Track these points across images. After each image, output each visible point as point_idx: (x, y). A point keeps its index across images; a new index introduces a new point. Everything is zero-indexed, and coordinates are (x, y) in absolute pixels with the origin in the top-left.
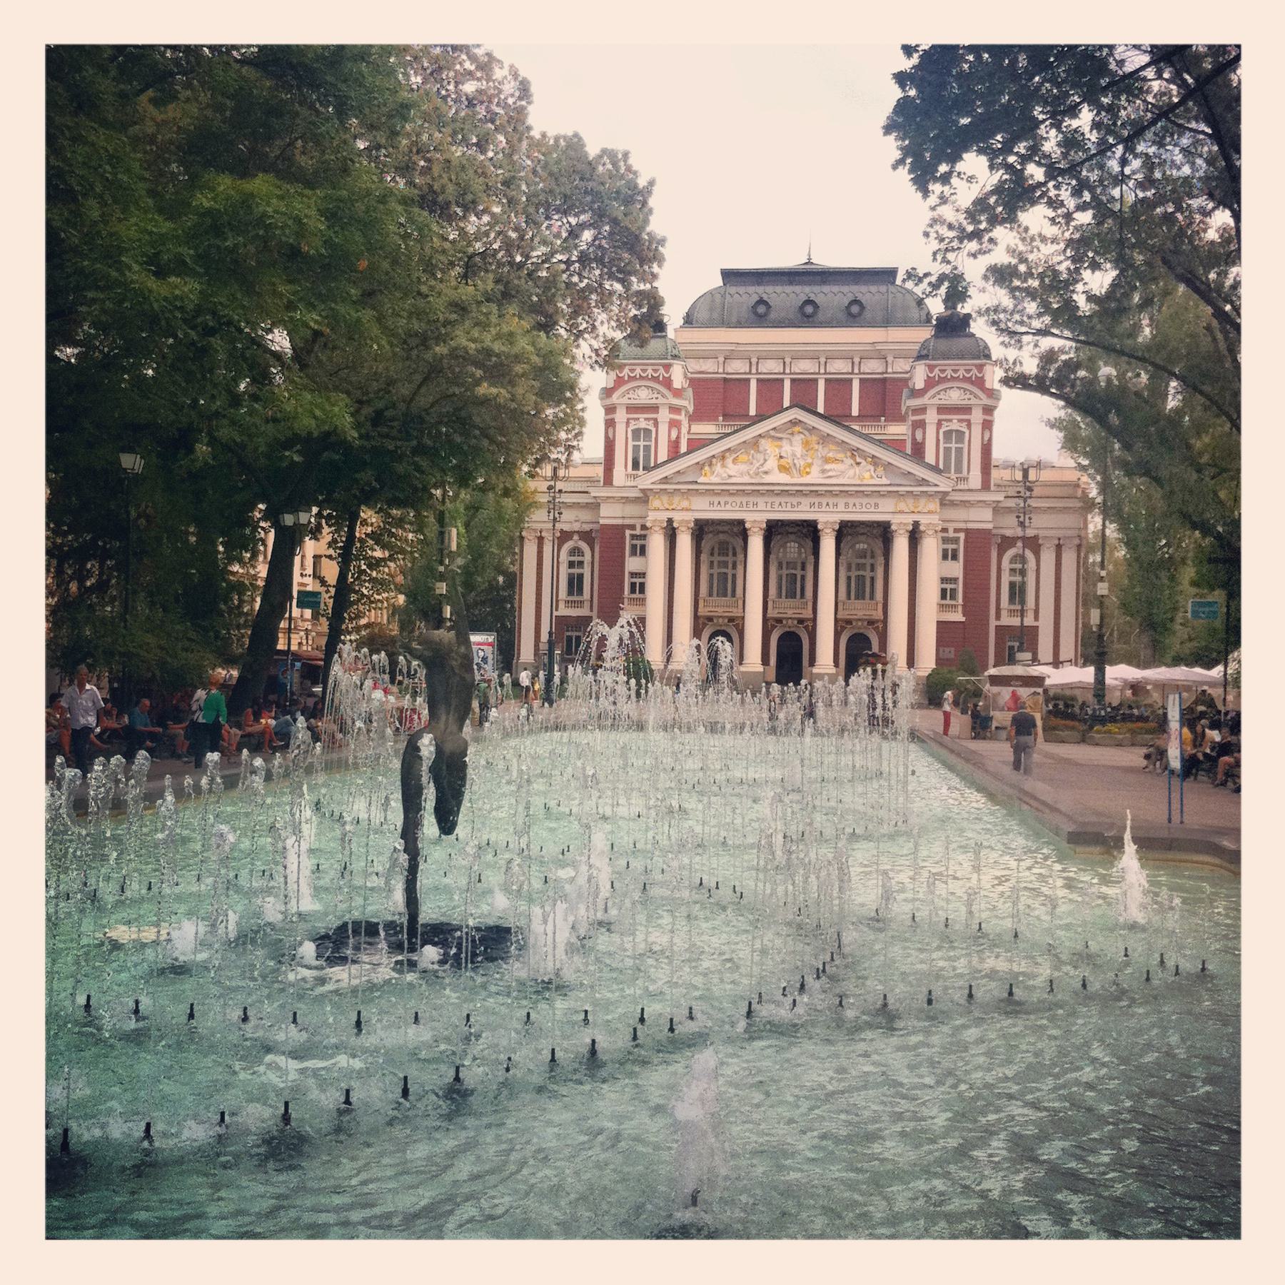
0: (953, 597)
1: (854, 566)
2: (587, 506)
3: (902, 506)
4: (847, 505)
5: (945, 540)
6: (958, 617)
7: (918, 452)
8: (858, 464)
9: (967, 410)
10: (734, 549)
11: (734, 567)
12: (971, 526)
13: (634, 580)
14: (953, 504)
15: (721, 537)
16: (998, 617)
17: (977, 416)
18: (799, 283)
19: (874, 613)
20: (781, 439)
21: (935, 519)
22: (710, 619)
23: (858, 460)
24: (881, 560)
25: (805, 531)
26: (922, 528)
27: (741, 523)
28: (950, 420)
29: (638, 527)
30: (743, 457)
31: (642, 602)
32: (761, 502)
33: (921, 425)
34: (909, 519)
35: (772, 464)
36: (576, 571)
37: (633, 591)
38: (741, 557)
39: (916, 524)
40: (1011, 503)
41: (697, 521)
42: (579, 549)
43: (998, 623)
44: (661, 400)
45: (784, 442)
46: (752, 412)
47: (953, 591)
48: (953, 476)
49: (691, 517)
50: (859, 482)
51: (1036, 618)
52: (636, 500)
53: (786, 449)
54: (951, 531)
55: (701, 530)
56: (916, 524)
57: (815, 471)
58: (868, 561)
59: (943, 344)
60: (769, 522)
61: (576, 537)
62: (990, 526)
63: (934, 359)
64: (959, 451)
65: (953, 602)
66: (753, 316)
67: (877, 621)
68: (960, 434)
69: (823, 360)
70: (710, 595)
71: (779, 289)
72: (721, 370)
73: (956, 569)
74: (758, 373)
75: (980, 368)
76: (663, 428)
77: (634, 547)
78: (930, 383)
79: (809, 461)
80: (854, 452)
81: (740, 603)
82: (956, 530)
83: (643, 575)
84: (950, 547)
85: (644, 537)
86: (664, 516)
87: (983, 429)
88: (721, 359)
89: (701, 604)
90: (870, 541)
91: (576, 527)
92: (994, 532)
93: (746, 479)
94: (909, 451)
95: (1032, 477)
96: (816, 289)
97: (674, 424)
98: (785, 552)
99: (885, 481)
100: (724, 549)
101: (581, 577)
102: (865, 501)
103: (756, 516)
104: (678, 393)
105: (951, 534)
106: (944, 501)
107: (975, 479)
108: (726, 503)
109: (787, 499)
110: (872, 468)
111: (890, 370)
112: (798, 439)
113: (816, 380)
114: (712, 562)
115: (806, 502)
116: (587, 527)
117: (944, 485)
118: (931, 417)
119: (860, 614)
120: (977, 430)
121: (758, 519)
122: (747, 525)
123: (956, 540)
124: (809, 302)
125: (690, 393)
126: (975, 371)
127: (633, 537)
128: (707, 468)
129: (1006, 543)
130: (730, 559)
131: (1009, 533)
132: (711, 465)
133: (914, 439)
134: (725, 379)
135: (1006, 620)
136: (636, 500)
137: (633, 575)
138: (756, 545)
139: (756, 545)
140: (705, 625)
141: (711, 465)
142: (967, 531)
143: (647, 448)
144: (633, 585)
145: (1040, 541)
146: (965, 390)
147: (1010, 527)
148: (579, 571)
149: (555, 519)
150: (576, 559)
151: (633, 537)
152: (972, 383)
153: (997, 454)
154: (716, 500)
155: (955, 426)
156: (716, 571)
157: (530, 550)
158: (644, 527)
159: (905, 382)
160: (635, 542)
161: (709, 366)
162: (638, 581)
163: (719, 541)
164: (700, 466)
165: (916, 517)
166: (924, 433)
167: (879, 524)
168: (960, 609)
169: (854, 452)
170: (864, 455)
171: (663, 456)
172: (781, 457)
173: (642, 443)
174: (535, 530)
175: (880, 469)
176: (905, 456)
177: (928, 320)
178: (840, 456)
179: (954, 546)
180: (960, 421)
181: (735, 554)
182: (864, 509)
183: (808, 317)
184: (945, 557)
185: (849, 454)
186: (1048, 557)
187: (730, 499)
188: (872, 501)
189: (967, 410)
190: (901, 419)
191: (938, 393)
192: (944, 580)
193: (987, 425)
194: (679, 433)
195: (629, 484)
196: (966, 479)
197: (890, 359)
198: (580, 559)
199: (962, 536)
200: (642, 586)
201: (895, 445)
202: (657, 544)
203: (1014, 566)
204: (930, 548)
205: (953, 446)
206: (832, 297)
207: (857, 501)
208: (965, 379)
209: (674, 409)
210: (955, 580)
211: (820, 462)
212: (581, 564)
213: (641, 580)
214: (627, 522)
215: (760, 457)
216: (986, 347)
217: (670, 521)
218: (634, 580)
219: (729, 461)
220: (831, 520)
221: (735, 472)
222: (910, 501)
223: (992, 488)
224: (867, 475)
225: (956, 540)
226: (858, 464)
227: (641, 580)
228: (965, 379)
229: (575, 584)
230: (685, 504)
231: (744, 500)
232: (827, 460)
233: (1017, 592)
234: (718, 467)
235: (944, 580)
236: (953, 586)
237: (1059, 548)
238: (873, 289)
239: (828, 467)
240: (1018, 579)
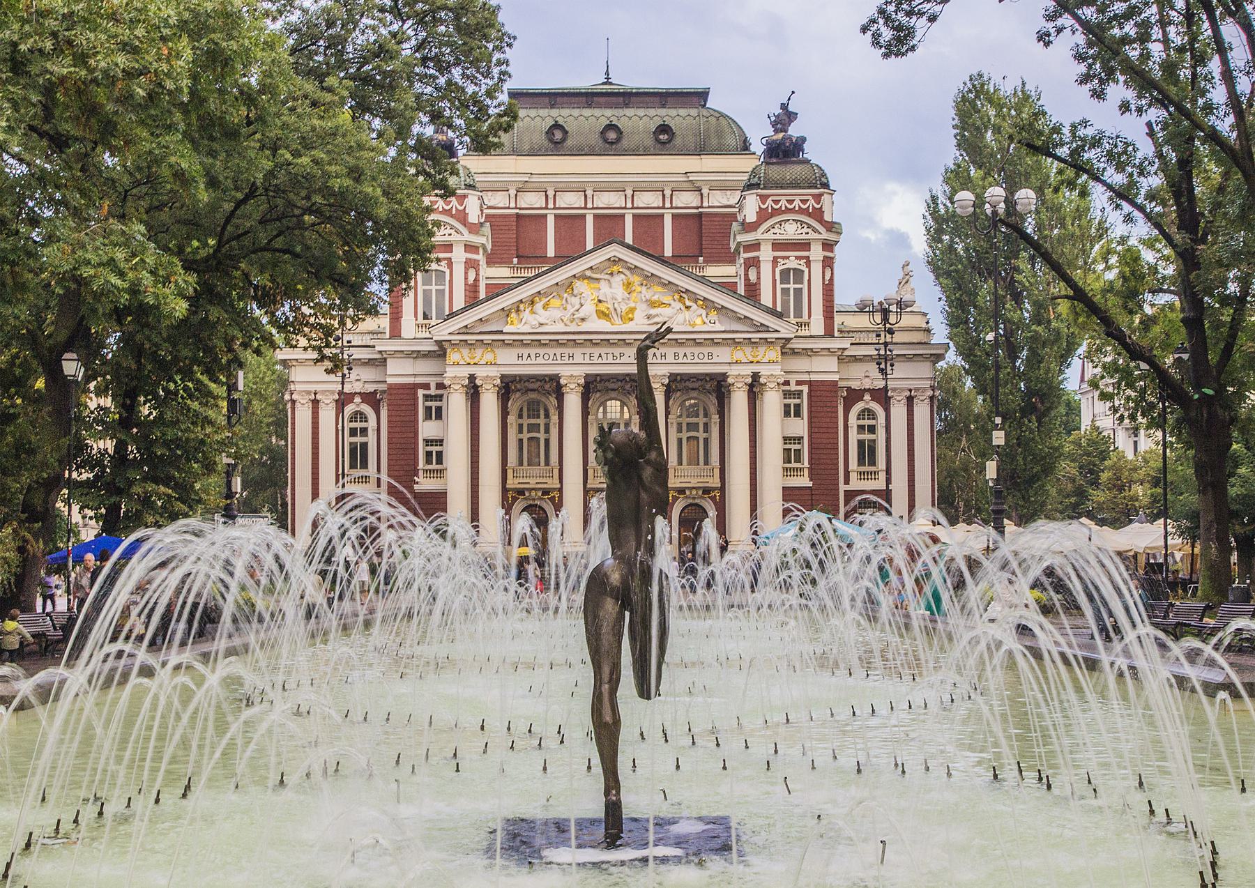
0: (798, 460)
1: (684, 428)
2: (369, 363)
3: (739, 355)
4: (676, 355)
5: (787, 394)
6: (804, 481)
7: (752, 293)
8: (688, 308)
9: (806, 245)
10: (547, 411)
11: (547, 431)
12: (814, 377)
13: (429, 449)
14: (794, 352)
15: (533, 396)
16: (847, 482)
17: (817, 253)
18: (600, 106)
19: (710, 480)
20: (598, 280)
21: (776, 370)
22: (521, 492)
23: (688, 303)
24: (715, 418)
25: (628, 387)
26: (762, 380)
27: (555, 379)
28: (788, 258)
29: (433, 386)
30: (555, 302)
31: (441, 473)
33: (754, 263)
34: (748, 370)
35: (589, 309)
36: (359, 439)
37: (429, 461)
38: (554, 418)
39: (755, 376)
40: (871, 351)
41: (503, 377)
42: (362, 414)
43: (848, 488)
44: (455, 237)
45: (602, 282)
46: (551, 253)
47: (798, 452)
48: (792, 320)
49: (495, 372)
50: (691, 329)
51: (888, 481)
52: (427, 355)
53: (605, 290)
54: (793, 383)
55: (508, 387)
56: (755, 376)
57: (639, 316)
58: (701, 420)
59: (776, 171)
60: (587, 376)
61: (358, 400)
62: (835, 377)
63: (764, 188)
64: (798, 292)
65: (798, 465)
66: (546, 143)
67: (714, 489)
68: (798, 273)
69: (629, 193)
70: (521, 464)
71: (576, 112)
72: (512, 205)
73: (800, 427)
74: (555, 208)
75: (818, 198)
76: (459, 270)
77: (428, 409)
78: (763, 216)
79: (632, 305)
80: (682, 293)
81: (556, 472)
82: (799, 383)
83: (440, 442)
84: (793, 402)
85: (439, 398)
86: (465, 372)
87: (824, 268)
88: (512, 192)
89: (510, 473)
90: (702, 396)
91: (358, 387)
92: (841, 384)
93: (560, 327)
94: (741, 290)
95: (892, 319)
96: (620, 112)
97: (470, 264)
98: (605, 412)
99: (718, 327)
100: (533, 409)
101: (364, 446)
102: (696, 350)
103: (572, 370)
104: (474, 229)
105: (793, 387)
106: (787, 349)
107: (817, 327)
109: (610, 350)
110: (704, 313)
111: (705, 204)
112: (618, 279)
113: (623, 216)
114: (521, 426)
116: (370, 388)
117: (785, 330)
118: (766, 254)
119: (694, 482)
120: (817, 268)
122: (562, 381)
123: (799, 394)
124: (611, 127)
125: (487, 229)
126: (812, 202)
127: (427, 397)
128: (513, 315)
129: (854, 396)
130: (541, 421)
131: (855, 385)
132: (518, 311)
133: (747, 279)
134: (518, 216)
135: (855, 484)
136: (427, 355)
137: (428, 442)
139: (573, 402)
140: (514, 499)
141: (518, 311)
142: (810, 383)
143: (440, 293)
144: (429, 454)
145: (890, 394)
147: (865, 376)
148: (363, 439)
149: (343, 376)
150: (358, 425)
151: (427, 397)
152: (809, 215)
153: (844, 298)
154: (525, 351)
155: (793, 264)
156: (525, 436)
157: (303, 416)
158: (440, 386)
159: (733, 217)
160: (429, 404)
161: (498, 200)
162: (434, 449)
163: (529, 396)
164: (506, 312)
165: (756, 368)
166: (759, 273)
167: (711, 377)
168: (806, 472)
169: (682, 293)
170: (695, 298)
171: (459, 303)
172: (600, 301)
173: (434, 288)
174: (309, 393)
175: (713, 315)
176: (740, 298)
177: (745, 147)
178: (667, 299)
179: (797, 401)
180: (797, 258)
181: (547, 416)
183: (612, 143)
184: (787, 413)
185: (677, 297)
186: (899, 411)
187: (542, 351)
188: (706, 350)
189: (806, 245)
190: (730, 259)
192: (786, 440)
193: (828, 263)
194: (477, 274)
195: (420, 335)
196: (807, 324)
197: (705, 191)
198: (363, 425)
199: (805, 388)
200: (439, 454)
201: (728, 288)
202: (457, 404)
203: (861, 422)
204: (772, 402)
205: (792, 286)
206: (639, 121)
207: (688, 350)
208: (801, 211)
209: (469, 248)
210: (799, 440)
211: (644, 306)
212: (364, 431)
213: (439, 448)
214: (419, 380)
215: (575, 301)
216: (824, 175)
217: (472, 378)
218: (429, 449)
219: (539, 306)
220: (659, 373)
221: (548, 318)
222: (748, 350)
223: (836, 334)
224: (699, 321)
225: (799, 394)
226: (688, 308)
227: (439, 448)
228: (801, 211)
229: (359, 456)
230: (489, 357)
231: (558, 351)
232: (652, 304)
233: (867, 453)
234: (526, 315)
235: (786, 440)
236: (797, 447)
237: (910, 400)
238: (683, 112)
239: (653, 311)
240: (867, 436)
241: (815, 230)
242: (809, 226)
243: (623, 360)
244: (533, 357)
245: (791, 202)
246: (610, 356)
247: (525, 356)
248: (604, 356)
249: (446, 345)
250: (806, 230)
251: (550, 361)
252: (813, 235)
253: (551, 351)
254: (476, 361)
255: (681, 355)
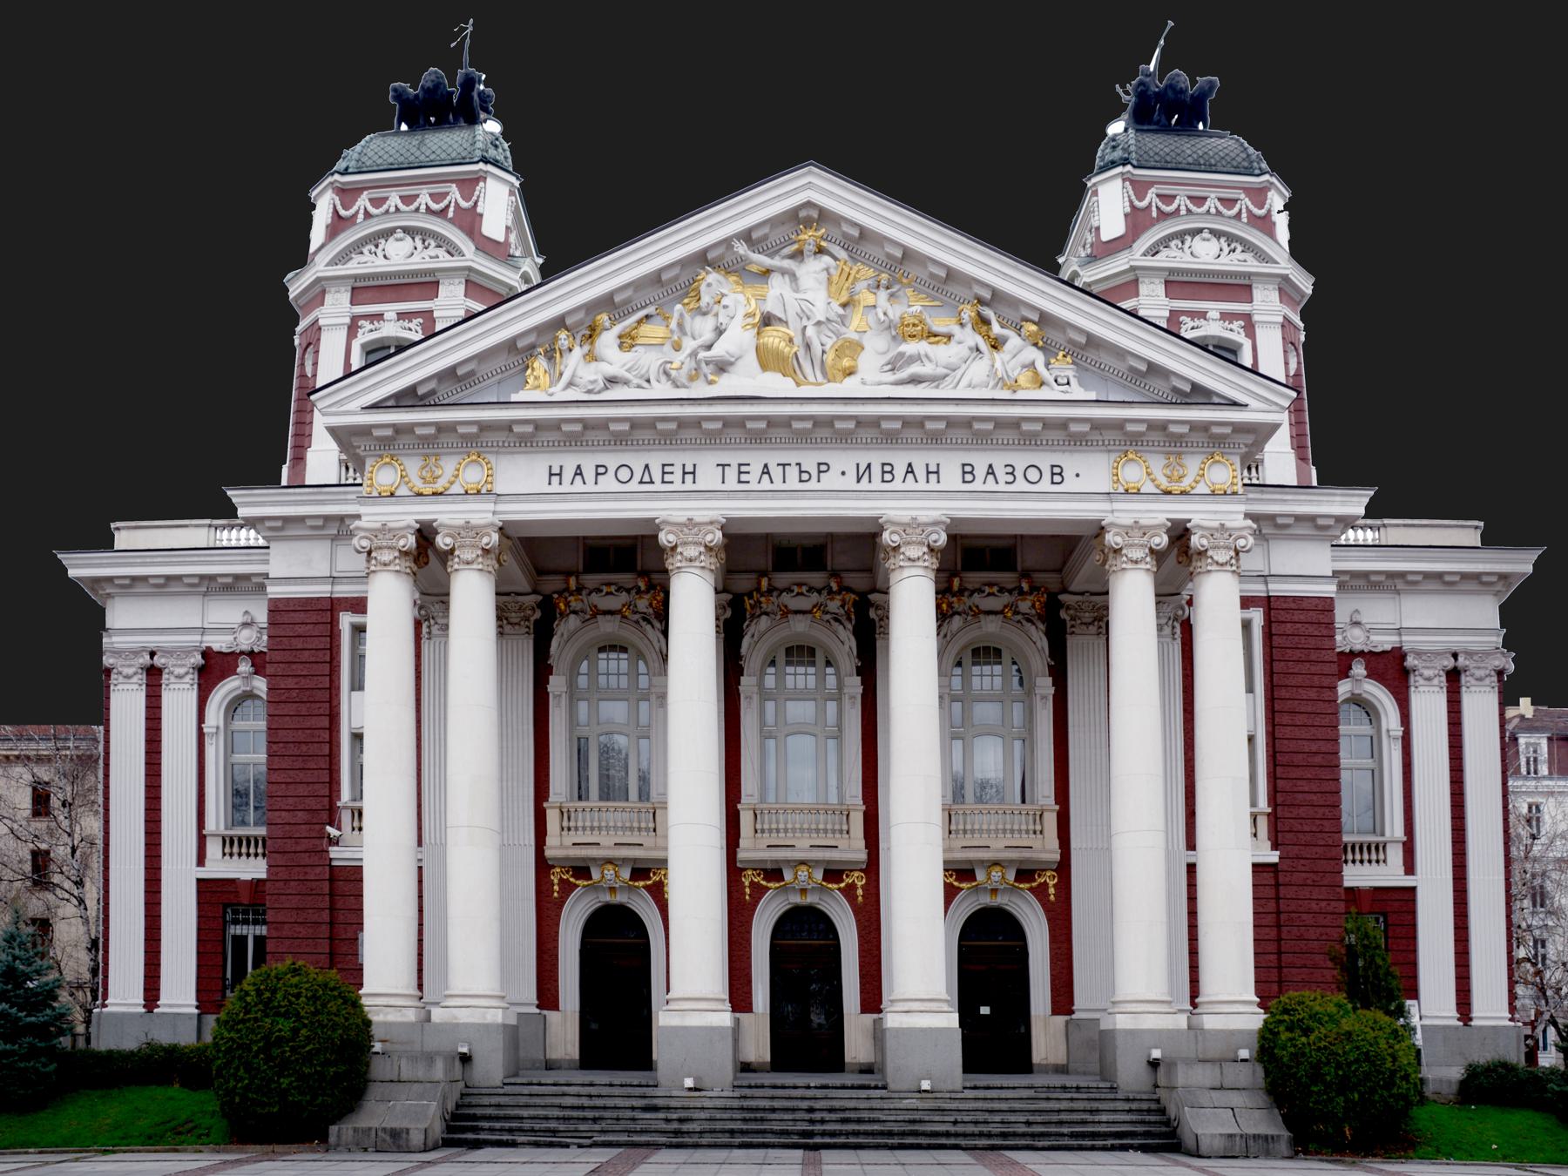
4: (967, 471)
28: (1202, 315)
32: (707, 466)
86: (407, 515)
102: (1020, 460)
103: (691, 504)
108: (600, 470)
109: (791, 457)
115: (844, 461)
121: (700, 517)
138: (693, 602)
146: (1231, 238)
154: (569, 462)
182: (1021, 485)
187: (611, 460)
188: (1045, 460)
191: (1165, 242)
207: (999, 460)
221: (626, 370)
230: (473, 476)
231: (656, 460)
241: (1262, 256)
242: (1248, 247)
243: (830, 481)
244: (589, 473)
245: (1199, 201)
246: (792, 472)
247: (568, 474)
248: (776, 472)
249: (361, 445)
250: (1238, 255)
251: (634, 486)
252: (1252, 265)
253: (637, 461)
254: (439, 487)
255: (980, 472)
